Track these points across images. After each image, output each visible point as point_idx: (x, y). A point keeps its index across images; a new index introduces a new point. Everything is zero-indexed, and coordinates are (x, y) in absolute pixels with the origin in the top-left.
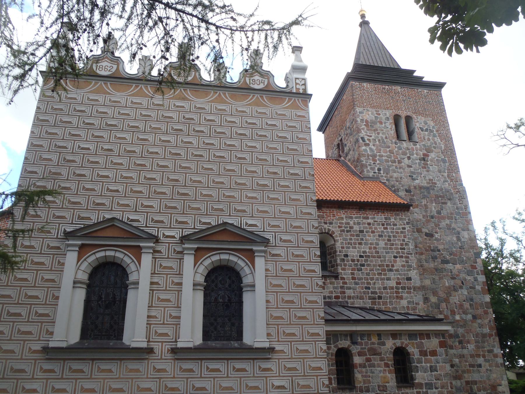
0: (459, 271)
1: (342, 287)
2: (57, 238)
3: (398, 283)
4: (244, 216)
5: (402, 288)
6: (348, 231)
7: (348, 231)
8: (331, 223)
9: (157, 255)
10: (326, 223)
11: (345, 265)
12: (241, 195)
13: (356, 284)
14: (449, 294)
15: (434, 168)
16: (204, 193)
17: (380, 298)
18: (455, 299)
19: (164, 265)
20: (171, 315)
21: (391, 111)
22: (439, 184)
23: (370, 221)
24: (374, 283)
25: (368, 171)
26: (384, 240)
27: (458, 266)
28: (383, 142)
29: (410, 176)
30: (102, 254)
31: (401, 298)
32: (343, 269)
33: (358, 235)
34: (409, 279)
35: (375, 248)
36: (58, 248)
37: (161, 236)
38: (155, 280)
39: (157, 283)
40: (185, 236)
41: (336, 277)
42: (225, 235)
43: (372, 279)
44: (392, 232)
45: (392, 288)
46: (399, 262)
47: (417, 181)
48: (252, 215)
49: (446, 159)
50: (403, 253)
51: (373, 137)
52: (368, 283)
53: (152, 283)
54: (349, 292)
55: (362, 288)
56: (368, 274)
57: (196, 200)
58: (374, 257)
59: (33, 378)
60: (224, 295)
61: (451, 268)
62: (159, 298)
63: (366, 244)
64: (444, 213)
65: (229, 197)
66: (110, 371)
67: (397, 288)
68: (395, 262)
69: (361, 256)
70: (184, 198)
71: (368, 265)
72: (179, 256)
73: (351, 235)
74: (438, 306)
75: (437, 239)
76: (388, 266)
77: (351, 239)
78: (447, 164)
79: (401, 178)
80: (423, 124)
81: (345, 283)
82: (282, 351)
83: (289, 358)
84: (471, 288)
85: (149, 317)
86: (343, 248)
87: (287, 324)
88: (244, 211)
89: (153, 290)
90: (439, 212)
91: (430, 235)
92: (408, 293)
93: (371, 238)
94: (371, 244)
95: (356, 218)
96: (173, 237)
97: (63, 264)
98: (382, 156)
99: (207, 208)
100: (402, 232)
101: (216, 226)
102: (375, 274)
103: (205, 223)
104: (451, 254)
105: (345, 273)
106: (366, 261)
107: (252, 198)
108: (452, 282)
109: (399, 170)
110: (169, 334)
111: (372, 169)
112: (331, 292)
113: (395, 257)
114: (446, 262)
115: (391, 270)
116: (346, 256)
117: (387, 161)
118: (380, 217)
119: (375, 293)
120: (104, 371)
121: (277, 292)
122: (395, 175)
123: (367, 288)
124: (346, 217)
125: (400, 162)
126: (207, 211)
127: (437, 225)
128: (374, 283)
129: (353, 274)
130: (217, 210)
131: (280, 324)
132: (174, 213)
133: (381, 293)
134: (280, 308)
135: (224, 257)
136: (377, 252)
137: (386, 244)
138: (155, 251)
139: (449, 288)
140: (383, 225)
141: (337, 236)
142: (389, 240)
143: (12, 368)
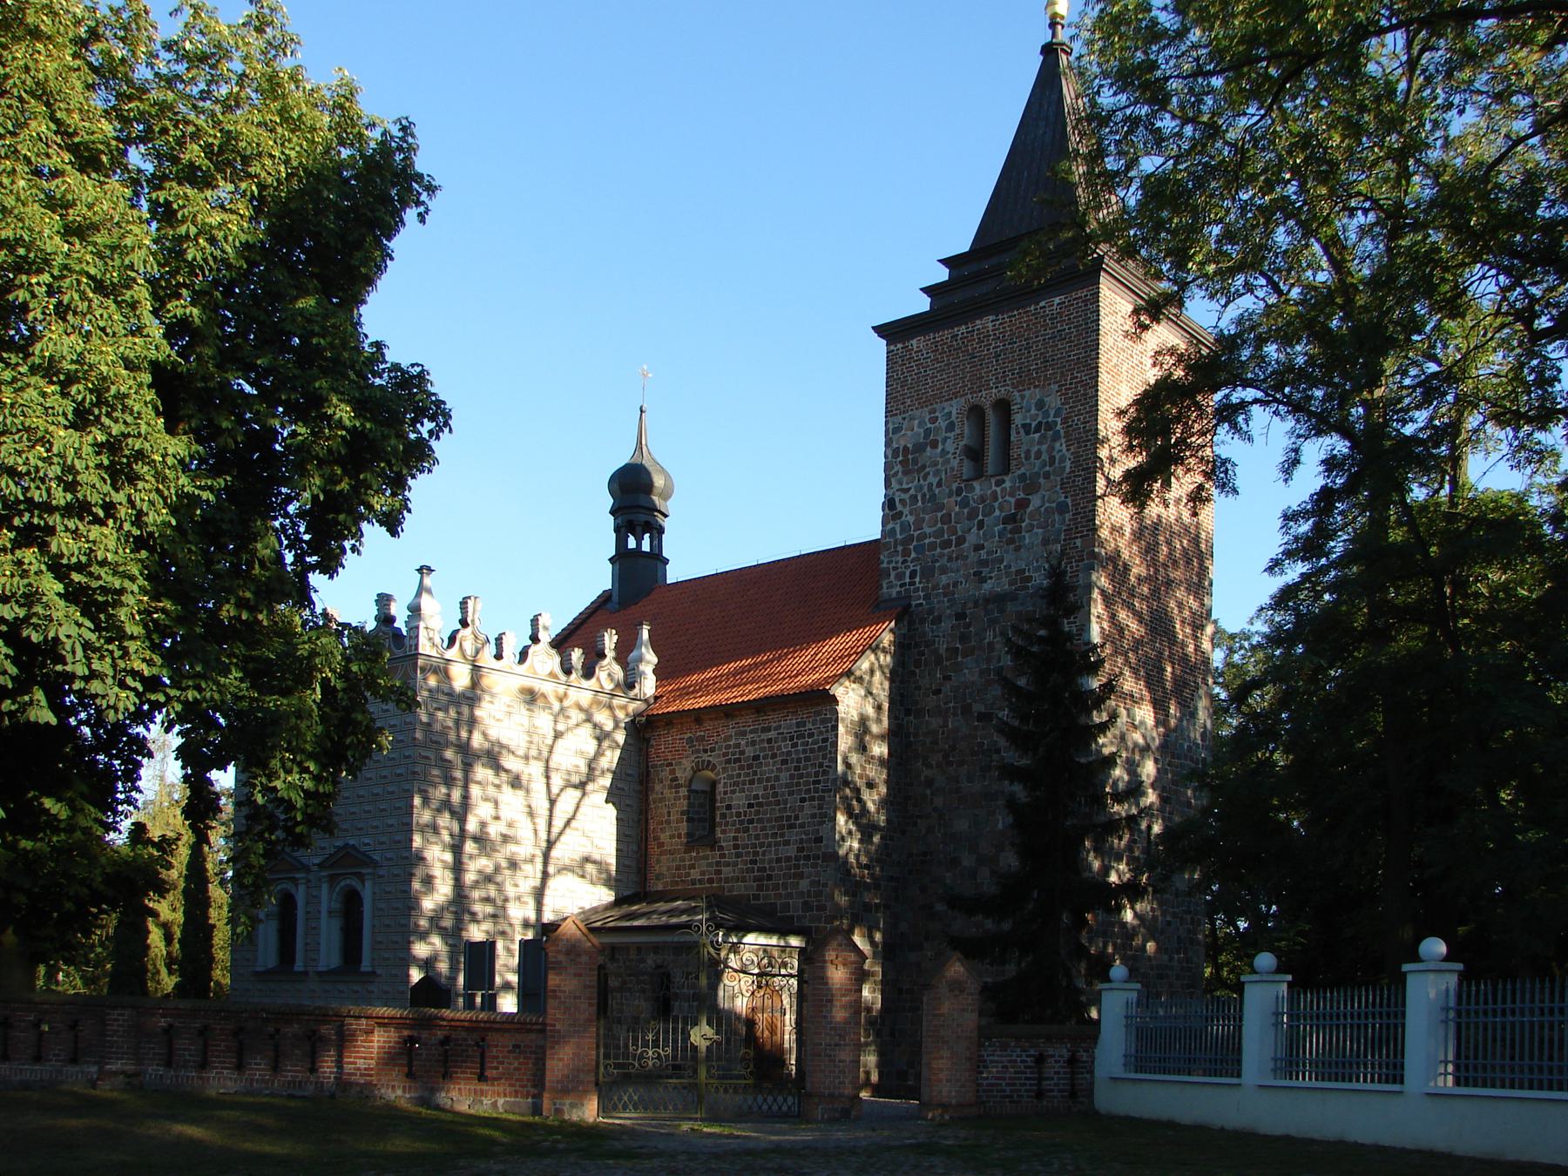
1: (718, 864)
3: (800, 850)
5: (807, 858)
6: (736, 760)
7: (736, 760)
8: (712, 750)
10: (705, 751)
11: (727, 824)
13: (738, 855)
15: (1032, 538)
17: (770, 877)
23: (772, 734)
25: (890, 586)
26: (788, 770)
31: (801, 876)
32: (724, 832)
33: (750, 766)
34: (819, 840)
35: (773, 787)
41: (713, 848)
43: (762, 845)
45: (788, 859)
46: (809, 809)
47: (987, 586)
49: (1069, 500)
50: (816, 791)
51: (912, 492)
56: (757, 837)
58: (769, 804)
67: (797, 859)
69: (750, 806)
73: (742, 768)
76: (789, 818)
77: (739, 775)
78: (1068, 516)
79: (955, 584)
92: (815, 866)
93: (769, 768)
94: (768, 780)
98: (924, 536)
102: (766, 836)
106: (757, 813)
109: (954, 565)
111: (900, 576)
112: (703, 873)
115: (791, 826)
116: (729, 807)
117: (932, 546)
118: (788, 723)
119: (764, 869)
122: (944, 579)
123: (754, 862)
125: (961, 541)
129: (735, 838)
133: (772, 869)
137: (792, 777)
140: (792, 739)
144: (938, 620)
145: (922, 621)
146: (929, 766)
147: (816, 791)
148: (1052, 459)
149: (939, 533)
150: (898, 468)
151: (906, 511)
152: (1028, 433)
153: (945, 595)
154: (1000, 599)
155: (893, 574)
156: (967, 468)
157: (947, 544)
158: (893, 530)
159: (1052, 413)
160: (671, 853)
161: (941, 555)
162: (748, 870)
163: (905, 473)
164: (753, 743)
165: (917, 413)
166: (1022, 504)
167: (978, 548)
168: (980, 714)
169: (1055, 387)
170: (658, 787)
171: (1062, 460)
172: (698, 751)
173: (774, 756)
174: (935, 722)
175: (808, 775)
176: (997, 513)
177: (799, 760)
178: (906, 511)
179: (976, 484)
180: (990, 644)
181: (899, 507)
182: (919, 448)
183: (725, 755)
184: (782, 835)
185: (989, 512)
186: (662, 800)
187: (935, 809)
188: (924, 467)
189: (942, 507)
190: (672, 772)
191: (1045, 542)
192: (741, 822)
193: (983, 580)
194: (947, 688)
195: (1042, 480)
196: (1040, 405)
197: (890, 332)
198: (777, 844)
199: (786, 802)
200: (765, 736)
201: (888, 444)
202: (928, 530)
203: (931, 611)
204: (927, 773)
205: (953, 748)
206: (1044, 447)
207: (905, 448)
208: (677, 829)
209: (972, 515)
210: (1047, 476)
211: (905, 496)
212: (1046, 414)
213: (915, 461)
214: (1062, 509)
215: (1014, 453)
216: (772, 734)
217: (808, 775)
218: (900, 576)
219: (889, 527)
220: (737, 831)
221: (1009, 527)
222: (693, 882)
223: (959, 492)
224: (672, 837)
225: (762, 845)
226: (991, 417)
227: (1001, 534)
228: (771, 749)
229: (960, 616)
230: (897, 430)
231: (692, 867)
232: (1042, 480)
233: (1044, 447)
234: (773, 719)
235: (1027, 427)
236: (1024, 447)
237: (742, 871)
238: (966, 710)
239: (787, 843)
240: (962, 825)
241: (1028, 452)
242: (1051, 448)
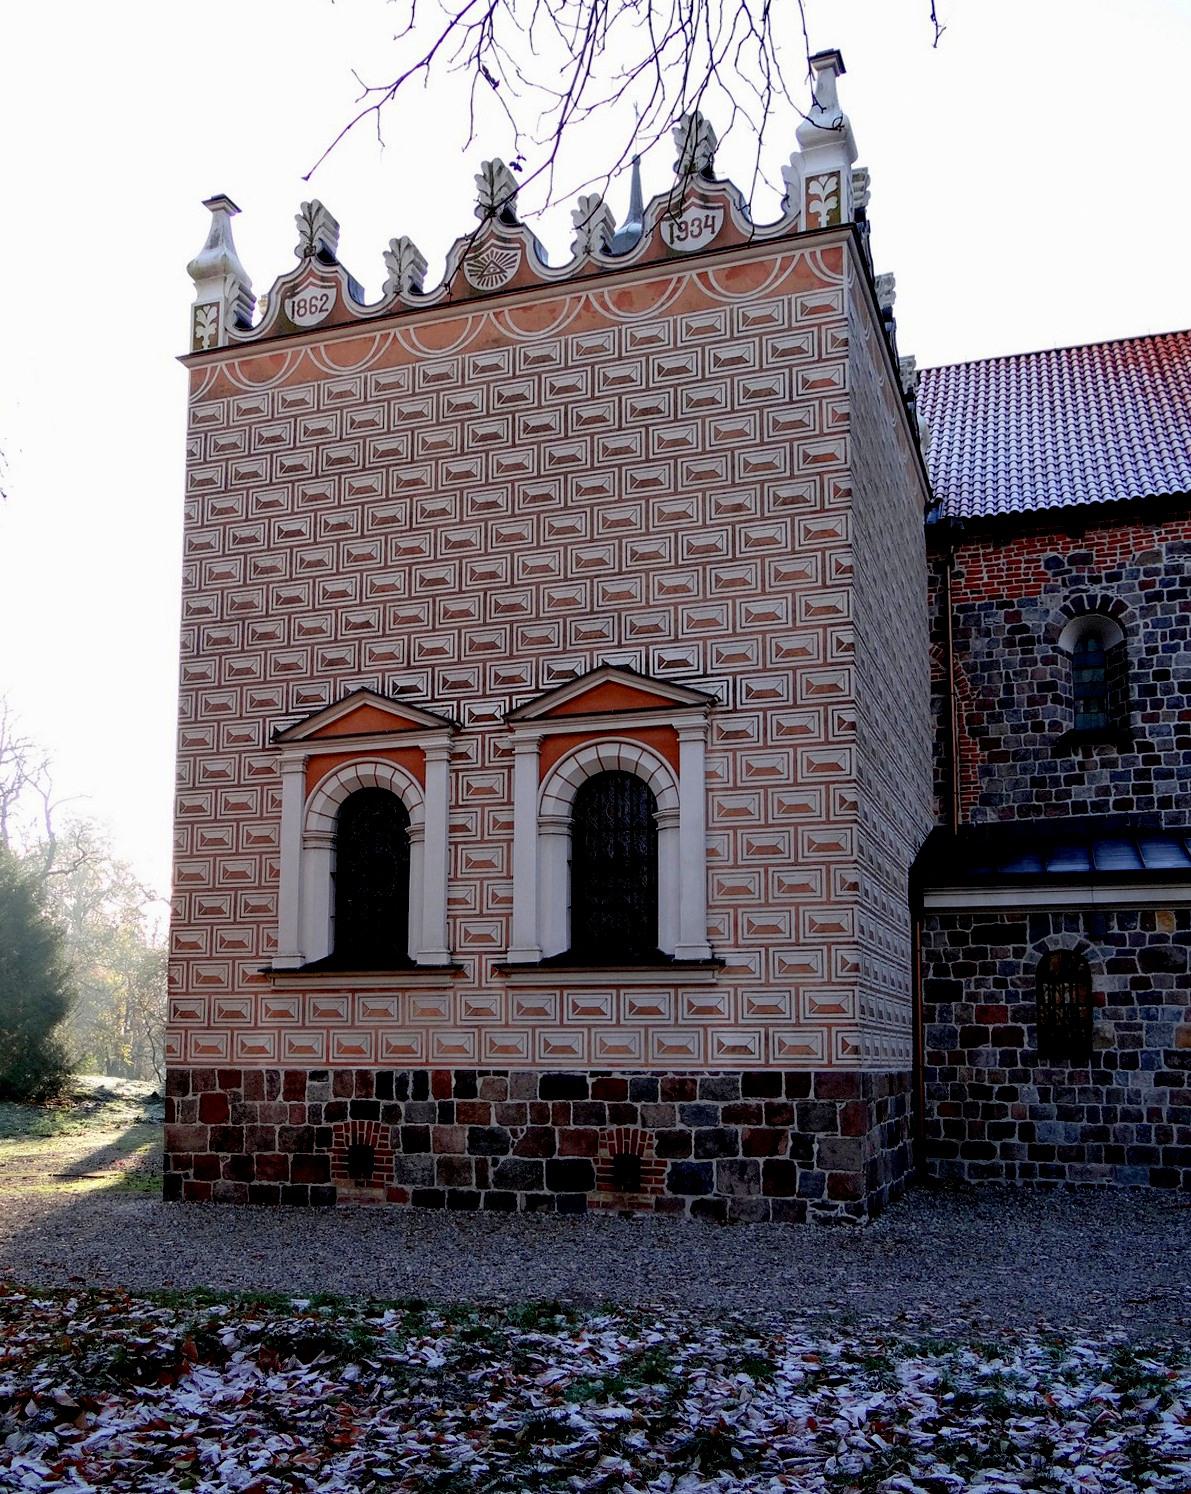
2: (264, 749)
4: (656, 643)
6: (1172, 596)
8: (1114, 577)
9: (459, 764)
10: (1096, 580)
11: (1157, 704)
12: (648, 587)
16: (557, 595)
19: (475, 785)
20: (495, 896)
30: (348, 774)
36: (269, 770)
37: (465, 717)
38: (459, 821)
39: (463, 828)
40: (519, 709)
41: (1125, 748)
42: (613, 696)
48: (676, 636)
53: (453, 828)
54: (1161, 788)
57: (538, 618)
59: (256, 1027)
60: (613, 841)
62: (469, 860)
65: (618, 596)
66: (386, 1012)
70: (510, 616)
72: (506, 761)
82: (745, 969)
83: (761, 985)
85: (450, 901)
86: (1151, 651)
87: (760, 905)
88: (657, 628)
89: (456, 844)
96: (492, 717)
97: (280, 804)
99: (565, 636)
101: (587, 675)
103: (561, 674)
107: (676, 589)
110: (493, 935)
112: (1105, 791)
120: (373, 1012)
121: (735, 829)
124: (1170, 550)
126: (565, 641)
130: (587, 636)
131: (740, 906)
132: (491, 660)
134: (743, 866)
135: (608, 751)
138: (455, 756)
141: (1133, 617)
143: (221, 1011)
160: (1017, 756)
170: (977, 644)
183: (1143, 586)
186: (994, 665)
222: (1079, 806)
224: (1016, 729)
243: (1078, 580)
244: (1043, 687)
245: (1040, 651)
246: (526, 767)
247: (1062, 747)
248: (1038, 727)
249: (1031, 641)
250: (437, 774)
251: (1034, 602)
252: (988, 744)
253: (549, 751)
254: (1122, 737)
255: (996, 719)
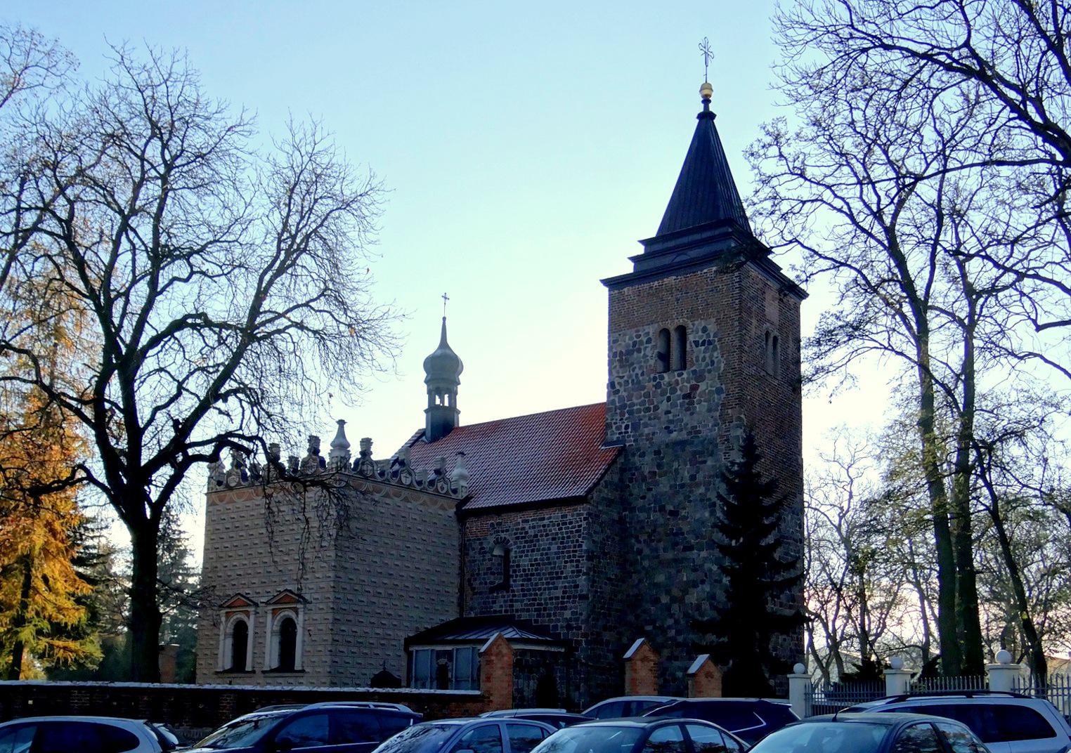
0: (705, 559)
1: (511, 601)
3: (564, 592)
5: (569, 597)
6: (523, 538)
7: (523, 538)
8: (507, 531)
10: (503, 531)
11: (517, 576)
13: (524, 595)
14: (685, 592)
15: (701, 408)
17: (545, 609)
18: (692, 598)
21: (656, 325)
22: (705, 433)
23: (546, 522)
24: (541, 595)
27: (704, 554)
28: (639, 382)
29: (666, 428)
31: (565, 608)
32: (514, 581)
33: (532, 541)
34: (577, 586)
35: (547, 554)
41: (508, 592)
43: (540, 589)
44: (567, 533)
45: (557, 598)
46: (570, 568)
49: (723, 386)
50: (574, 556)
51: (625, 378)
52: (536, 594)
54: (517, 605)
55: (529, 600)
56: (536, 584)
58: (544, 564)
61: (695, 556)
63: (538, 550)
64: (700, 477)
67: (563, 598)
68: (565, 567)
69: (532, 565)
71: (538, 574)
73: (526, 542)
74: (668, 608)
75: (685, 518)
76: (557, 573)
78: (723, 396)
80: (700, 333)
81: (514, 596)
84: (716, 581)
90: (693, 477)
91: (674, 514)
92: (574, 602)
93: (543, 543)
94: (544, 549)
95: (532, 520)
98: (634, 405)
100: (577, 531)
102: (543, 584)
104: (697, 538)
105: (517, 584)
106: (537, 570)
108: (693, 576)
109: (652, 422)
112: (501, 606)
113: (566, 562)
114: (690, 548)
115: (560, 578)
116: (518, 566)
117: (639, 411)
118: (555, 515)
119: (541, 604)
122: (646, 431)
123: (535, 600)
125: (656, 408)
127: (687, 498)
128: (541, 595)
129: (522, 585)
136: (548, 559)
137: (559, 548)
139: (687, 583)
140: (558, 525)
142: (562, 543)
144: (643, 455)
145: (634, 455)
146: (639, 542)
147: (574, 556)
148: (713, 363)
149: (643, 403)
150: (617, 364)
151: (622, 389)
152: (697, 346)
153: (647, 440)
154: (682, 444)
155: (614, 427)
156: (660, 366)
157: (648, 409)
158: (614, 401)
159: (712, 335)
160: (481, 593)
161: (645, 416)
162: (531, 605)
163: (621, 367)
164: (534, 527)
165: (629, 332)
166: (695, 388)
167: (668, 412)
168: (670, 511)
169: (714, 320)
170: (471, 553)
171: (719, 362)
172: (498, 532)
173: (547, 535)
174: (643, 516)
175: (570, 547)
176: (679, 392)
177: (563, 538)
178: (622, 389)
179: (665, 375)
180: (676, 470)
181: (618, 387)
182: (629, 353)
183: (515, 534)
184: (554, 583)
185: (674, 391)
186: (475, 561)
187: (644, 568)
188: (633, 364)
189: (644, 388)
190: (481, 544)
191: (709, 410)
192: (527, 575)
193: (671, 432)
194: (649, 495)
195: (706, 374)
196: (705, 330)
197: (614, 284)
198: (550, 589)
199: (555, 563)
200: (541, 523)
201: (610, 349)
202: (635, 401)
203: (638, 449)
204: (637, 546)
205: (654, 531)
206: (707, 355)
207: (621, 352)
208: (484, 579)
209: (663, 394)
210: (709, 371)
211: (622, 381)
212: (708, 335)
213: (627, 360)
214: (719, 391)
215: (688, 358)
216: (546, 522)
217: (570, 547)
218: (618, 428)
219: (612, 398)
220: (523, 580)
221: (687, 401)
222: (495, 612)
223: (655, 379)
225: (540, 589)
226: (674, 337)
227: (682, 405)
228: (545, 531)
229: (657, 453)
230: (615, 342)
231: (494, 602)
232: (706, 374)
233: (707, 355)
234: (546, 513)
235: (697, 344)
236: (695, 355)
237: (526, 605)
238: (662, 509)
239: (556, 588)
240: (660, 578)
241: (697, 357)
242: (711, 356)
243: (498, 532)
244: (488, 569)
245: (488, 556)
246: (270, 617)
247: (492, 590)
248: (486, 583)
249: (485, 552)
250: (252, 617)
251: (485, 539)
252: (473, 589)
253: (274, 612)
254: (505, 586)
255: (475, 580)
